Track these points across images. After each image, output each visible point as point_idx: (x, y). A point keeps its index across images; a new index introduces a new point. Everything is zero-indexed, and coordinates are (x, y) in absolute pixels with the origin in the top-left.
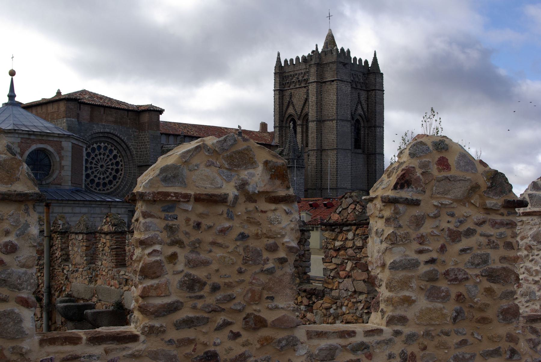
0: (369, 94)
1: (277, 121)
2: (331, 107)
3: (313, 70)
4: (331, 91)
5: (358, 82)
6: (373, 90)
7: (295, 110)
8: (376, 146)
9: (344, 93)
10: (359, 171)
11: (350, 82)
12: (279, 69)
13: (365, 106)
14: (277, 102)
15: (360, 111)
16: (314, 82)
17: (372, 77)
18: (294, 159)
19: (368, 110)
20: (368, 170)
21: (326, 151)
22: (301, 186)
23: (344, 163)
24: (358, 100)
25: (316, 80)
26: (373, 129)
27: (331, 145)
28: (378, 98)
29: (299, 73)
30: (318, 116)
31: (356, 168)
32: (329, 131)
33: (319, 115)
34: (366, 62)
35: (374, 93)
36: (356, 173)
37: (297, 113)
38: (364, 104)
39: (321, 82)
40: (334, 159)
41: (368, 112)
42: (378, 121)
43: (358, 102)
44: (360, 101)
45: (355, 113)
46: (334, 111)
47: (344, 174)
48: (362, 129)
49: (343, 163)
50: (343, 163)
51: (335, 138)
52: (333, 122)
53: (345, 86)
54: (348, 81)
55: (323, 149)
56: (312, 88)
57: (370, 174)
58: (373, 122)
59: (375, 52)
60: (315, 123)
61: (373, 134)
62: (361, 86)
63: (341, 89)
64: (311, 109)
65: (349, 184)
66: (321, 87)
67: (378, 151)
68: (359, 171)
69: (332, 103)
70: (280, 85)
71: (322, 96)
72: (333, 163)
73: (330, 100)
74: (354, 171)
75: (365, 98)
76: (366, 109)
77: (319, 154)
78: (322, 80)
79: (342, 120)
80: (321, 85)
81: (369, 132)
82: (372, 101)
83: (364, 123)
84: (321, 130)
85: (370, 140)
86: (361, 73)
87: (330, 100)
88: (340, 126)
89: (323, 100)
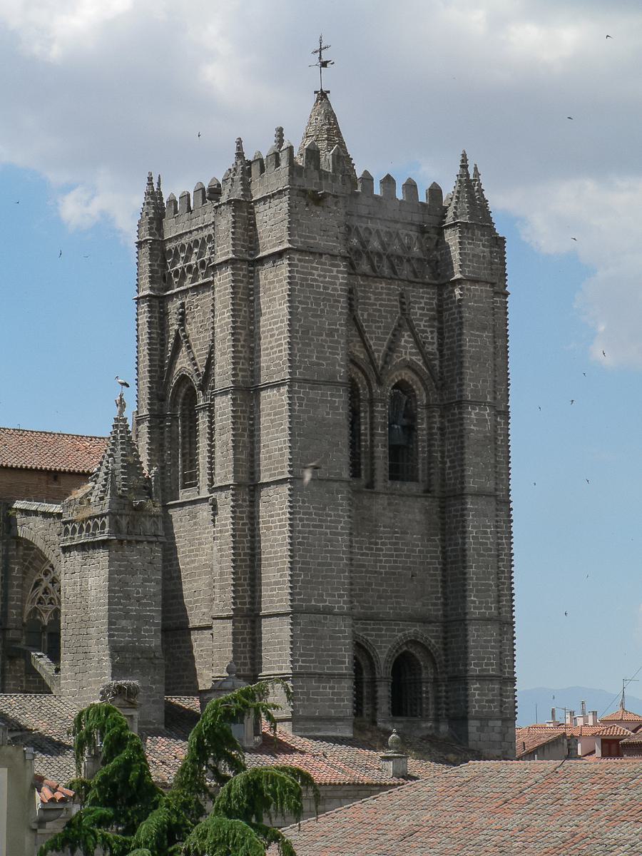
0: (445, 296)
1: (144, 400)
3: (226, 221)
4: (275, 288)
5: (399, 257)
7: (193, 359)
9: (320, 293)
10: (408, 556)
11: (345, 258)
12: (150, 229)
13: (431, 338)
14: (145, 338)
15: (407, 350)
18: (121, 515)
19: (441, 351)
20: (444, 553)
22: (146, 605)
23: (321, 527)
24: (400, 318)
25: (231, 256)
26: (456, 411)
28: (469, 307)
29: (203, 239)
30: (240, 374)
31: (396, 544)
33: (241, 370)
34: (435, 192)
36: (395, 562)
37: (197, 370)
38: (425, 332)
39: (248, 261)
41: (442, 356)
43: (400, 325)
44: (409, 322)
45: (386, 362)
47: (319, 564)
48: (422, 413)
49: (314, 526)
50: (314, 526)
53: (322, 270)
54: (336, 252)
56: (223, 280)
59: (464, 155)
61: (457, 430)
62: (414, 272)
63: (307, 280)
64: (220, 350)
65: (341, 596)
66: (252, 278)
68: (408, 556)
69: (277, 329)
70: (151, 282)
71: (252, 307)
73: (274, 317)
74: (385, 555)
75: (432, 310)
76: (435, 346)
77: (244, 500)
78: (251, 255)
79: (314, 384)
80: (250, 272)
82: (453, 320)
83: (427, 395)
84: (252, 419)
86: (414, 228)
87: (274, 317)
88: (304, 402)
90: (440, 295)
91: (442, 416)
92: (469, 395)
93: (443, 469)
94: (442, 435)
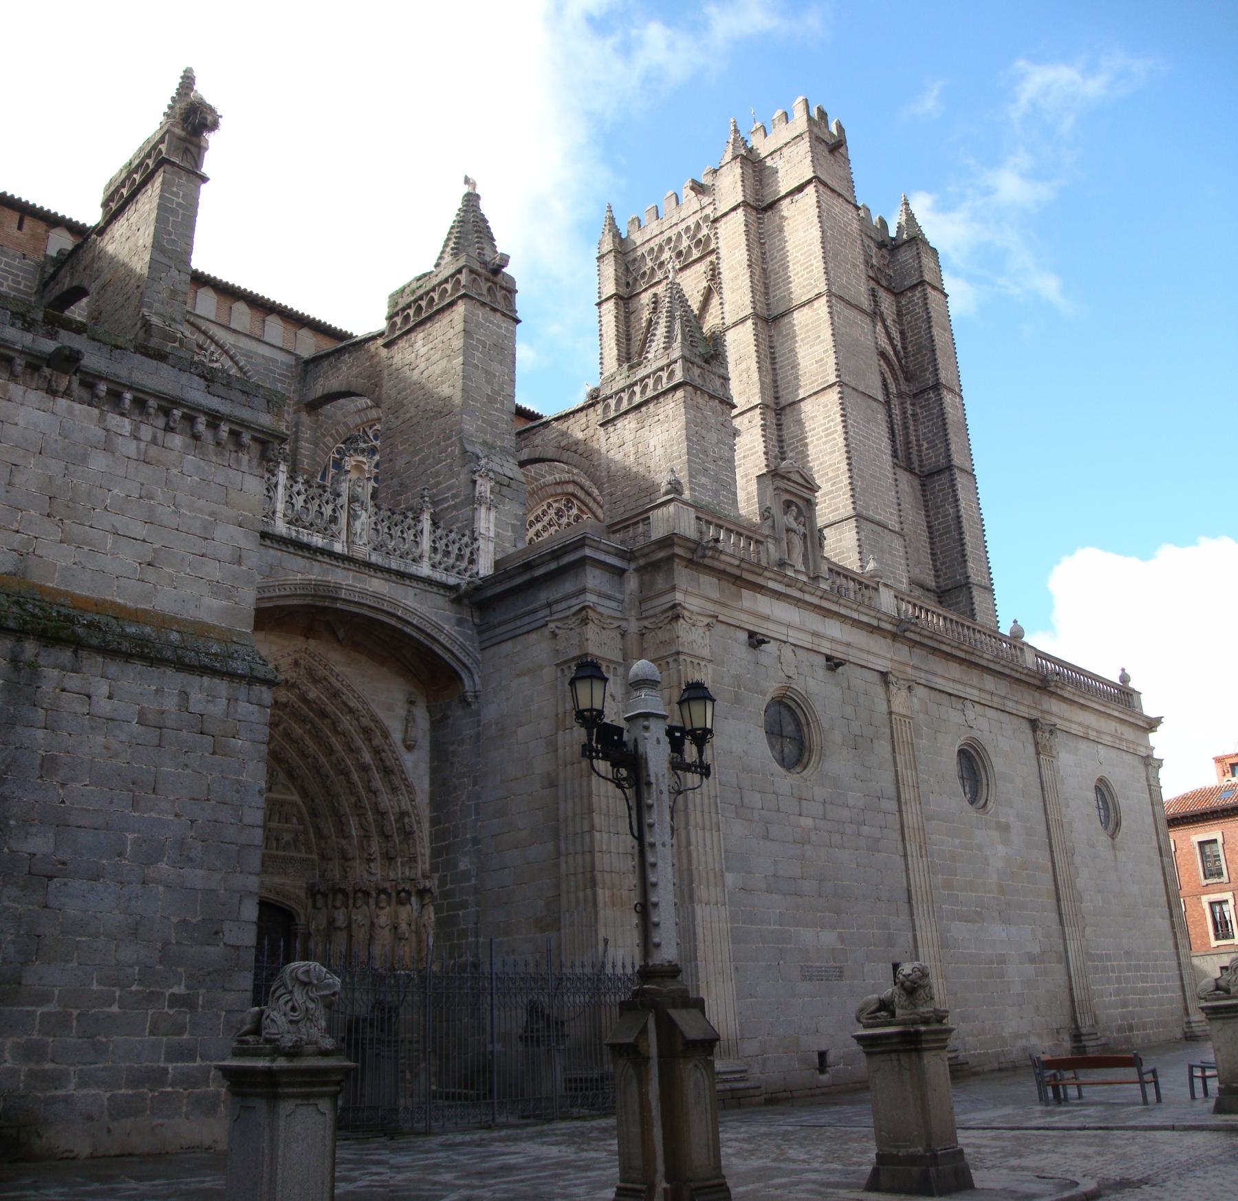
0: (903, 303)
2: (801, 265)
6: (914, 287)
8: (948, 445)
16: (734, 209)
17: (905, 256)
27: (816, 381)
35: (918, 295)
40: (832, 420)
42: (943, 375)
46: (815, 271)
50: (863, 436)
55: (781, 406)
57: (940, 535)
58: (928, 375)
61: (935, 411)
66: (760, 223)
67: (957, 460)
72: (827, 436)
73: (797, 246)
80: (759, 218)
81: (919, 411)
82: (916, 320)
85: (924, 434)
87: (797, 246)
89: (769, 259)
90: (898, 302)
91: (913, 405)
92: (943, 381)
93: (920, 451)
94: (915, 421)
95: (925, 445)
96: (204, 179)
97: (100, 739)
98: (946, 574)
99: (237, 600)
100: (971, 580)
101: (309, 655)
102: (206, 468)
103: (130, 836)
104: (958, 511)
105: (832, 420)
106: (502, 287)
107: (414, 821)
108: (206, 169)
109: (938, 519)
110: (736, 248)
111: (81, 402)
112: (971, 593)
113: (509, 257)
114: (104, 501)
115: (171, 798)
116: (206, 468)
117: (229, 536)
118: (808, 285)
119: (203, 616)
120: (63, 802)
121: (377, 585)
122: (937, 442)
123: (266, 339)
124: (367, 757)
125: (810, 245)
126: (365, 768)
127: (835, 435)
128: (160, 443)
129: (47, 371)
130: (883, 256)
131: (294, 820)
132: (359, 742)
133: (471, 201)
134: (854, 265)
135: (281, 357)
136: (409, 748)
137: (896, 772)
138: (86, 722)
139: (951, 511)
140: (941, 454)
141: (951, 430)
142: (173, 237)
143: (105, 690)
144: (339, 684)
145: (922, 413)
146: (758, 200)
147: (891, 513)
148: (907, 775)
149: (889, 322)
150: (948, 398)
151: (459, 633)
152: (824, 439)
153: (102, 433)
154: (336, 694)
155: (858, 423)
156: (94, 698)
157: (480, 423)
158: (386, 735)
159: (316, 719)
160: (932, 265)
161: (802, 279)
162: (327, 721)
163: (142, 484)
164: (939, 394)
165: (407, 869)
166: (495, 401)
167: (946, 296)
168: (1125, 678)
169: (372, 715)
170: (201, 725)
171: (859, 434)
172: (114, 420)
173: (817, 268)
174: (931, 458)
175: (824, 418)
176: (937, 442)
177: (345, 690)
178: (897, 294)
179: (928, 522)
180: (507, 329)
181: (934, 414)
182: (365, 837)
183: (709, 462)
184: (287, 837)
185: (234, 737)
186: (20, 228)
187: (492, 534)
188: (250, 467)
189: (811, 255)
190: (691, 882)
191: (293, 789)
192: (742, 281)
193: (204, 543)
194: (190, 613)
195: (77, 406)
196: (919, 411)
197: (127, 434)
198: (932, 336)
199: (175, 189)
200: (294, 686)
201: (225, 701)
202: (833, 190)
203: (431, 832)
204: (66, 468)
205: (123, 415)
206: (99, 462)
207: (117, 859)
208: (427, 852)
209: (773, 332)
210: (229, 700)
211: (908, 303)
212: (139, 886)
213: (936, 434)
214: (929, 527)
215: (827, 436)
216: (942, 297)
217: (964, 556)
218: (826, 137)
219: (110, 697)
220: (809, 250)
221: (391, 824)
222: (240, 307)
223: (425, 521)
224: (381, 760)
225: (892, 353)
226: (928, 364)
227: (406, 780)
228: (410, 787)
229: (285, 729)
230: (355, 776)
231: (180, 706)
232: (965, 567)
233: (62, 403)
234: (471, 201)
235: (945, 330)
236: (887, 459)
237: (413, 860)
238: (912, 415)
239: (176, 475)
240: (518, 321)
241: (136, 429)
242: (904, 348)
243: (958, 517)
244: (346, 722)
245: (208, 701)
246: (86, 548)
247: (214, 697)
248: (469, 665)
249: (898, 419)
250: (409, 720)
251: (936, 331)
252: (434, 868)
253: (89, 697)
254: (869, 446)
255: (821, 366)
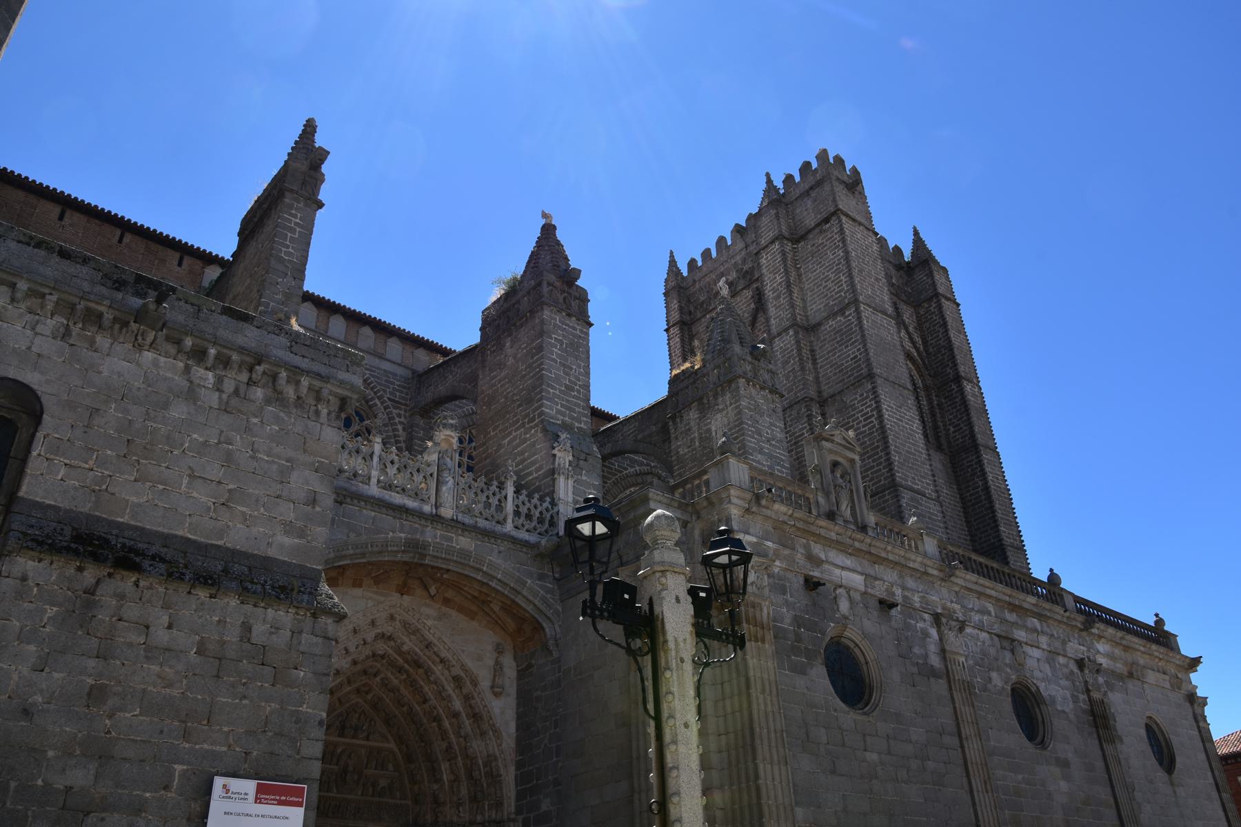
0: (922, 313)
2: (832, 282)
17: (920, 275)
21: (838, 398)
32: (838, 343)
40: (869, 406)
42: (961, 369)
50: (897, 419)
51: (859, 350)
52: (847, 313)
58: (948, 371)
60: (791, 332)
61: (957, 400)
66: (796, 252)
72: (865, 420)
80: (795, 248)
81: (943, 401)
85: (950, 420)
87: (827, 267)
90: (917, 313)
95: (952, 429)
96: (320, 205)
97: (155, 668)
98: (980, 538)
99: (309, 538)
100: (1004, 542)
101: (404, 610)
102: (286, 419)
103: (179, 768)
104: (987, 483)
105: (869, 406)
106: (576, 298)
107: (500, 765)
108: (322, 196)
109: (969, 491)
110: (777, 273)
111: (167, 355)
112: (1005, 553)
113: (580, 271)
114: (182, 445)
115: (226, 729)
116: (286, 419)
117: (303, 481)
118: (839, 297)
119: (272, 553)
120: (109, 732)
121: (465, 542)
122: (962, 425)
123: (388, 356)
124: (458, 705)
125: (838, 264)
126: (456, 715)
127: (873, 419)
128: (242, 395)
129: (134, 326)
130: (900, 276)
131: (391, 767)
132: (450, 688)
133: (548, 230)
134: (877, 279)
135: (400, 371)
136: (497, 695)
137: (955, 708)
138: (142, 652)
139: (980, 483)
140: (966, 435)
141: (973, 413)
142: (290, 250)
143: (165, 620)
144: (431, 636)
145: (946, 403)
146: (792, 234)
147: (928, 484)
148: (965, 711)
149: (911, 329)
150: (968, 387)
151: (541, 587)
152: (863, 423)
153: (185, 384)
154: (429, 646)
155: (892, 408)
156: (152, 629)
157: (559, 407)
158: (475, 683)
159: (410, 670)
160: (944, 280)
161: (833, 293)
162: (421, 671)
163: (222, 432)
164: (960, 386)
165: (494, 812)
166: (572, 389)
167: (958, 305)
168: (1160, 622)
169: (463, 665)
170: (261, 655)
171: (893, 417)
172: (199, 372)
173: (845, 282)
174: (958, 439)
175: (862, 406)
176: (962, 425)
177: (435, 641)
178: (916, 305)
179: (961, 495)
180: (581, 331)
181: (955, 403)
182: (455, 781)
183: (763, 442)
184: (383, 783)
185: (296, 669)
186: (180, 264)
187: (570, 500)
188: (329, 420)
189: (839, 272)
190: (761, 815)
191: (389, 736)
192: (784, 299)
193: (279, 486)
194: (261, 550)
195: (162, 359)
196: (943, 401)
197: (210, 386)
198: (949, 338)
199: (293, 212)
200: (390, 638)
201: (289, 634)
202: (854, 220)
203: (516, 776)
204: (147, 413)
205: (207, 369)
206: (179, 411)
207: (163, 792)
208: (513, 794)
209: (813, 339)
210: (293, 633)
211: (926, 313)
212: (184, 821)
213: (961, 419)
214: (962, 499)
215: (865, 420)
216: (955, 306)
217: (995, 521)
218: (845, 179)
219: (170, 627)
220: (837, 269)
221: (480, 770)
222: (367, 331)
223: (509, 487)
224: (470, 706)
225: (916, 354)
226: (948, 361)
227: (494, 725)
228: (497, 733)
229: (382, 679)
230: (446, 724)
231: (242, 637)
232: (998, 531)
233: (148, 356)
234: (548, 230)
235: (960, 332)
236: (919, 436)
237: (499, 805)
238: (938, 405)
239: (256, 424)
240: (591, 325)
241: (220, 380)
242: (926, 351)
243: (987, 488)
244: (438, 670)
245: (271, 633)
246: (161, 487)
247: (278, 629)
248: (551, 616)
249: (926, 409)
250: (498, 669)
251: (952, 334)
252: (519, 811)
253: (147, 627)
254: (903, 427)
255: (855, 363)
